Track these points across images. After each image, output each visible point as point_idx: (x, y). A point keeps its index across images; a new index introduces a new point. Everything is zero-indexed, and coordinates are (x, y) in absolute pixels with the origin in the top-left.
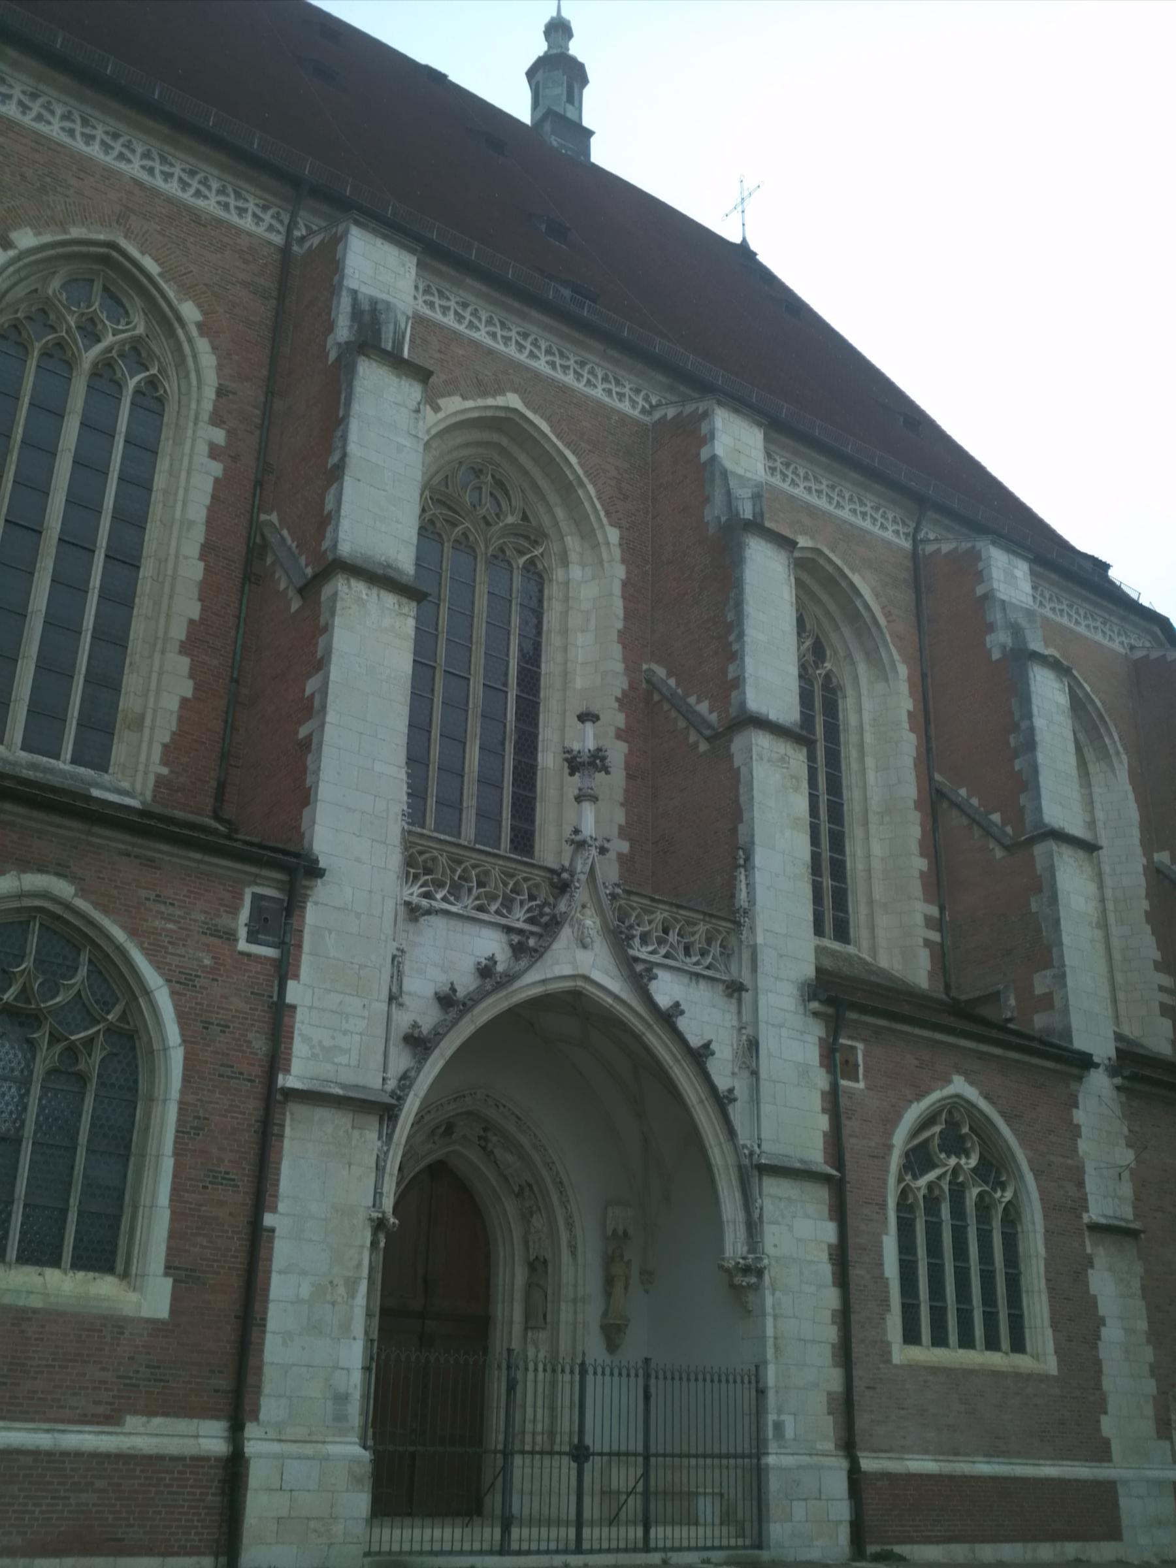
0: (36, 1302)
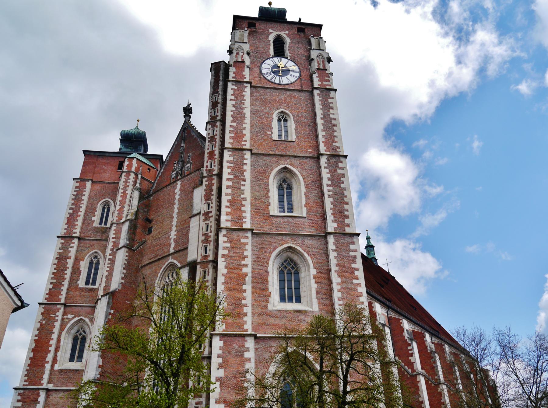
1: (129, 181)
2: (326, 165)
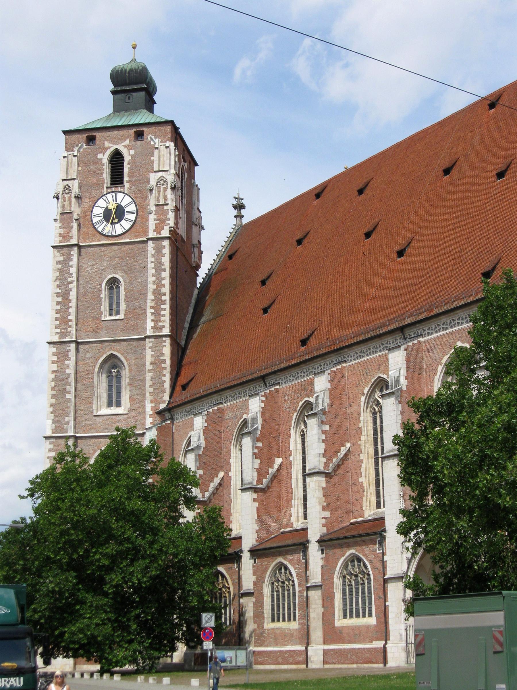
0: (361, 624)
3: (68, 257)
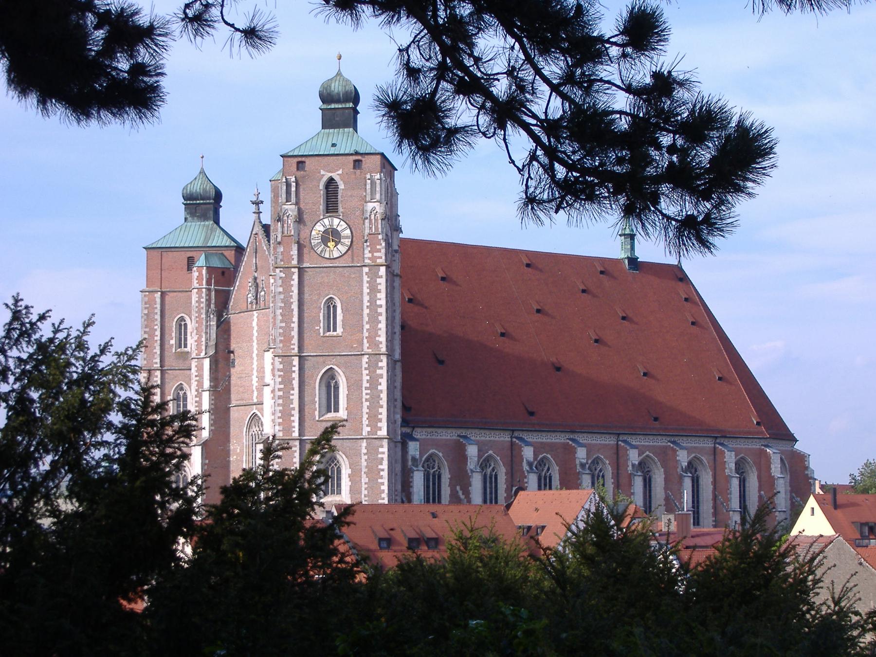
1: (202, 300)
2: (367, 366)
3: (289, 277)
